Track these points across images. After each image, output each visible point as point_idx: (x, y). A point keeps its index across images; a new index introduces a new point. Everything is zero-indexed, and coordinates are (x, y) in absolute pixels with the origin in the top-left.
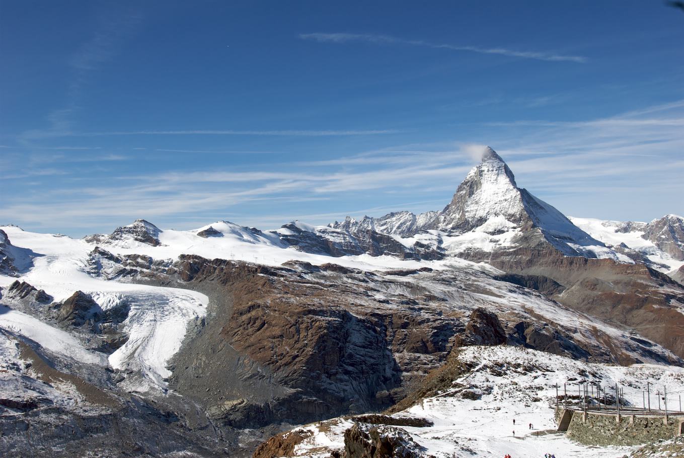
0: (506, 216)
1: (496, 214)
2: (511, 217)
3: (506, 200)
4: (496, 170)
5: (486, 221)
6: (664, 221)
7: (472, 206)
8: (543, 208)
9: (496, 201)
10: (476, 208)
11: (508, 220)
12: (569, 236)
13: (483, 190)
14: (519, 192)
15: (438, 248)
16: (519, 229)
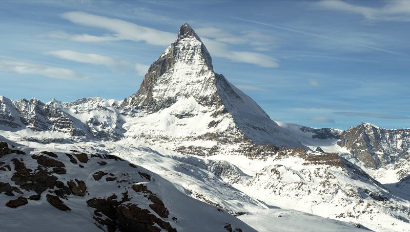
0: (197, 98)
1: (187, 96)
2: (203, 100)
3: (199, 82)
4: (192, 49)
5: (174, 102)
6: (361, 128)
7: (161, 85)
8: (239, 97)
9: (189, 82)
10: (165, 87)
11: (199, 103)
12: (263, 128)
13: (175, 69)
14: (213, 75)
15: (116, 127)
16: (211, 113)
